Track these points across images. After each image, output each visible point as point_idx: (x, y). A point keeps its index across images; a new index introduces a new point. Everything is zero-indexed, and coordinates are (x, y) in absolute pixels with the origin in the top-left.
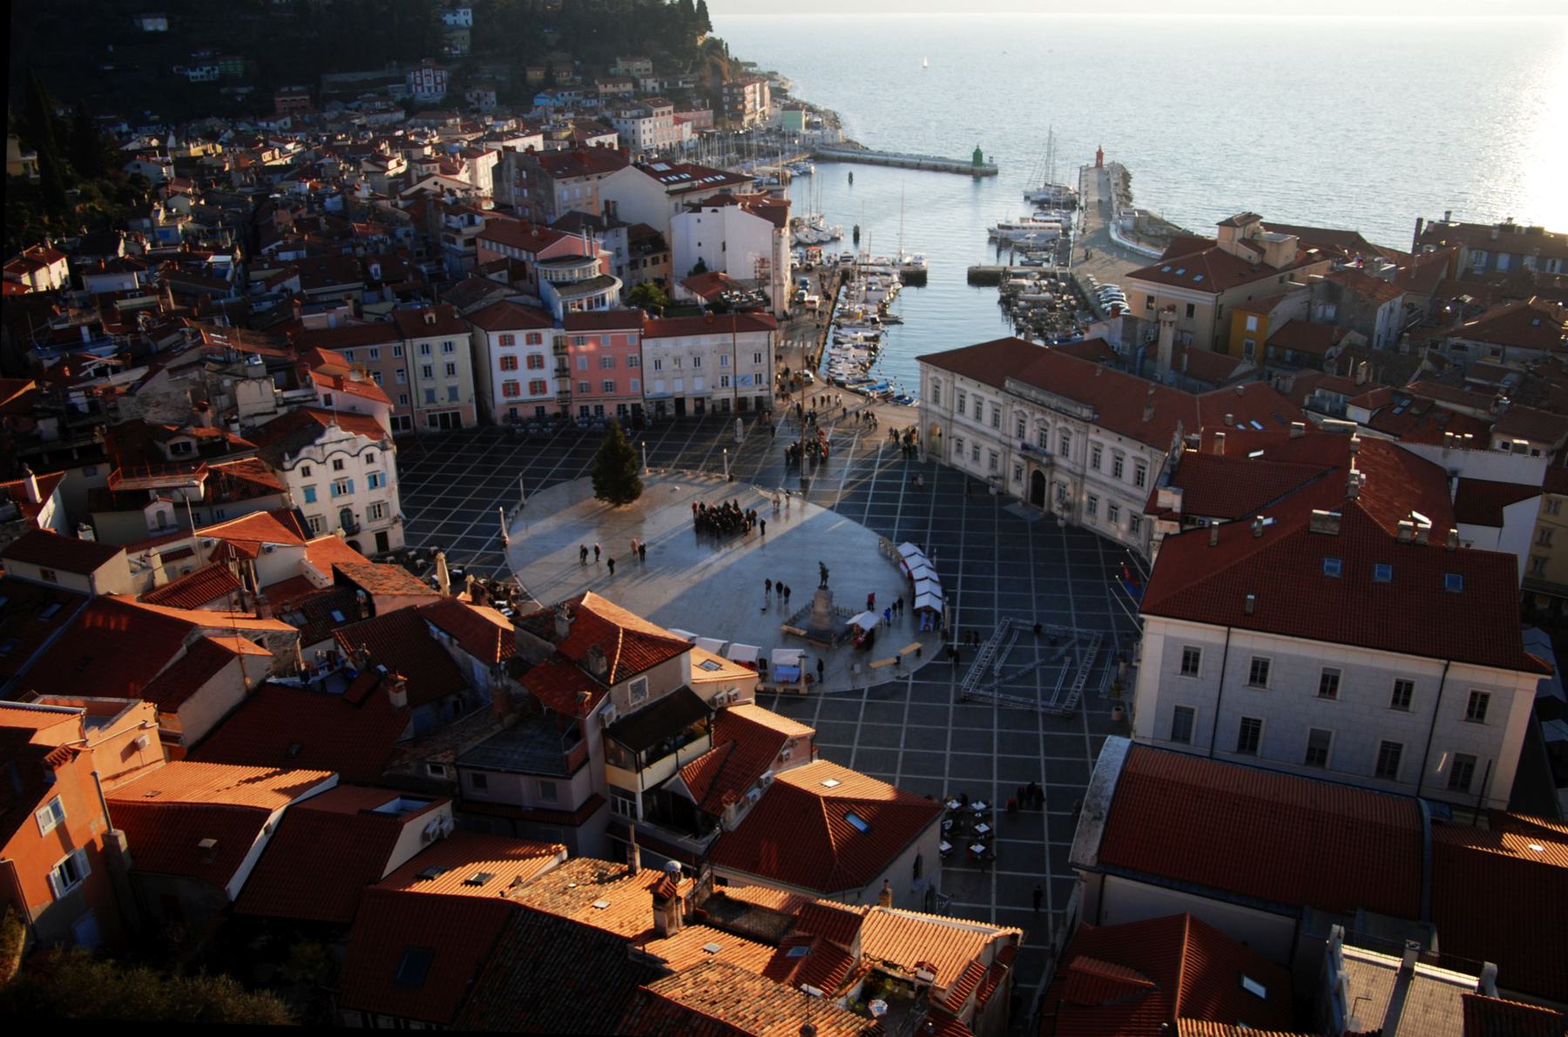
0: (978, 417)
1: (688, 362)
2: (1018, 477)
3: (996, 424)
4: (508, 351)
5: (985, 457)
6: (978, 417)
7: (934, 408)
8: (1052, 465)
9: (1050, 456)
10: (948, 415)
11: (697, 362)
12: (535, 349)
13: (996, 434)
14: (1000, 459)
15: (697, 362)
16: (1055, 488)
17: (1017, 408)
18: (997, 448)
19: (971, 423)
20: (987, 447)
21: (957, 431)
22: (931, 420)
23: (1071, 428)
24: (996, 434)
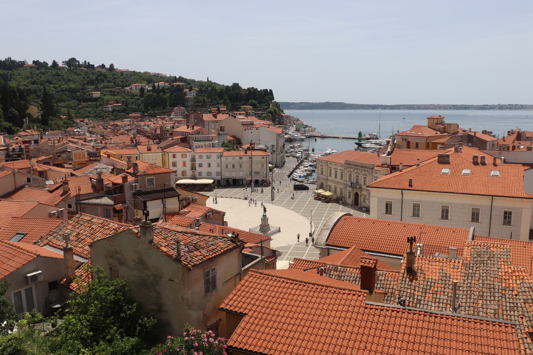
0: (336, 177)
1: (237, 166)
2: (350, 197)
3: (342, 179)
4: (174, 160)
5: (338, 190)
6: (336, 177)
7: (322, 176)
8: (361, 188)
9: (360, 186)
10: (326, 177)
11: (241, 166)
12: (184, 159)
13: (342, 181)
14: (343, 191)
15: (241, 166)
16: (362, 197)
17: (348, 170)
18: (343, 187)
19: (334, 179)
20: (339, 187)
21: (329, 183)
22: (321, 181)
23: (367, 173)
24: (342, 181)
